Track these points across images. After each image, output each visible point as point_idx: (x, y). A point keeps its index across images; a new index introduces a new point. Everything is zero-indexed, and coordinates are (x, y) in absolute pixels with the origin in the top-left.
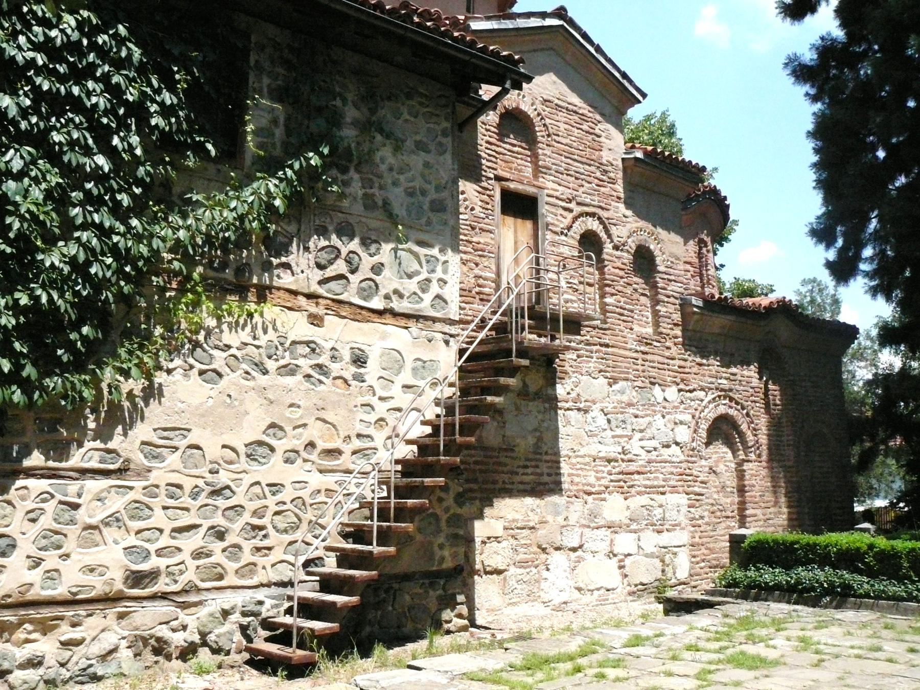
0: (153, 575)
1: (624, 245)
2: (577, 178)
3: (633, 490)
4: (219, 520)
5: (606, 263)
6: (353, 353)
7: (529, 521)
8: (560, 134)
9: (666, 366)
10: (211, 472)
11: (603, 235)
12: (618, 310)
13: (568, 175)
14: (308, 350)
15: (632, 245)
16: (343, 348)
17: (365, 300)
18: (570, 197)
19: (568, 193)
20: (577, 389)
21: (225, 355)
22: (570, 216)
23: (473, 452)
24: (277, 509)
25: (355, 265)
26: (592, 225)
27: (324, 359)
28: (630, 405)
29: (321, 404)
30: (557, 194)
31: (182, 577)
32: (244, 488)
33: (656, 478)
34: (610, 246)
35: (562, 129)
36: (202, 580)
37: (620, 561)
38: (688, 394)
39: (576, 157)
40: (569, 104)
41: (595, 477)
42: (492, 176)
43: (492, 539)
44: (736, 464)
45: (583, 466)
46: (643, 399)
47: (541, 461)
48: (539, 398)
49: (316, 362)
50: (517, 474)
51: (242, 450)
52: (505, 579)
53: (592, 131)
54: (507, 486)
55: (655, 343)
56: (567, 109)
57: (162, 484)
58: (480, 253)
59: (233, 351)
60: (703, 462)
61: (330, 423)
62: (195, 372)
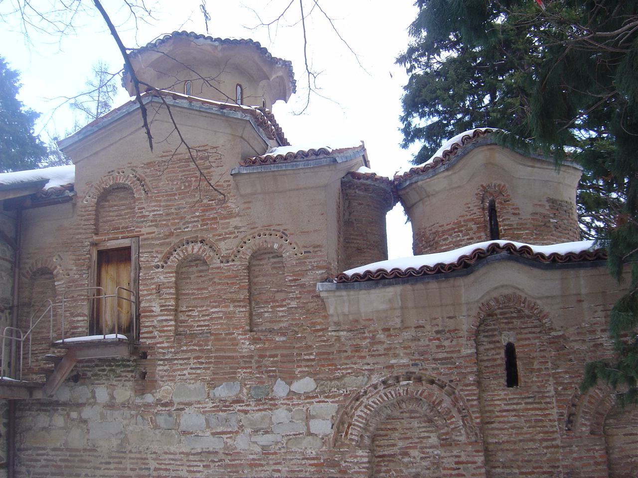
19: (166, 231)
22: (166, 249)
23: (59, 452)
26: (193, 249)
28: (239, 401)
33: (279, 471)
34: (219, 261)
41: (188, 471)
45: (172, 462)
48: (124, 407)
50: (100, 469)
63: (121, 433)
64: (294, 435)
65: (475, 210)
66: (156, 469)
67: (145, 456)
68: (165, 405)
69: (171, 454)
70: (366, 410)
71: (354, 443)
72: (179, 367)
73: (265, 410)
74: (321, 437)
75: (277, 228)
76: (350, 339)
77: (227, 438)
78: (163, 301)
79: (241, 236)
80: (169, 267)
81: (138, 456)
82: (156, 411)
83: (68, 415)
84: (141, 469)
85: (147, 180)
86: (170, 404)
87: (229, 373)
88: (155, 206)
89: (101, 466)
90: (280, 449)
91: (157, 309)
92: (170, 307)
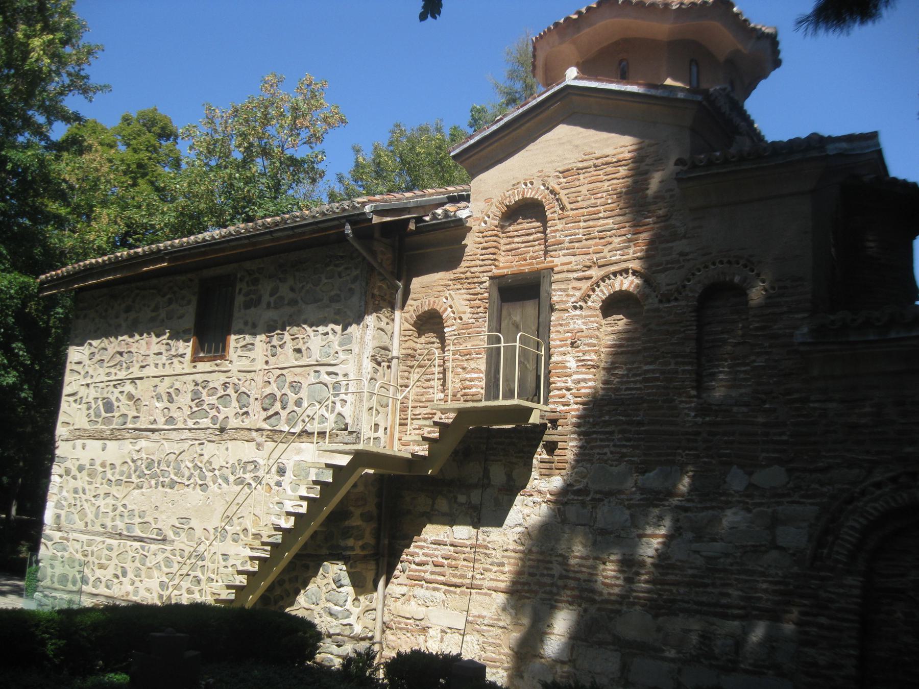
2: (600, 239)
8: (579, 199)
13: (587, 240)
18: (588, 264)
20: (585, 481)
21: (211, 474)
22: (589, 283)
26: (622, 284)
30: (569, 267)
34: (656, 300)
39: (601, 215)
40: (597, 159)
43: (453, 630)
50: (490, 570)
55: (735, 409)
56: (595, 166)
57: (178, 549)
63: (520, 525)
64: (753, 546)
67: (548, 558)
70: (861, 520)
71: (840, 566)
72: (598, 443)
73: (712, 508)
74: (791, 552)
78: (581, 354)
80: (590, 308)
83: (456, 498)
85: (563, 192)
88: (573, 228)
89: (491, 567)
90: (731, 565)
91: (572, 364)
92: (590, 363)
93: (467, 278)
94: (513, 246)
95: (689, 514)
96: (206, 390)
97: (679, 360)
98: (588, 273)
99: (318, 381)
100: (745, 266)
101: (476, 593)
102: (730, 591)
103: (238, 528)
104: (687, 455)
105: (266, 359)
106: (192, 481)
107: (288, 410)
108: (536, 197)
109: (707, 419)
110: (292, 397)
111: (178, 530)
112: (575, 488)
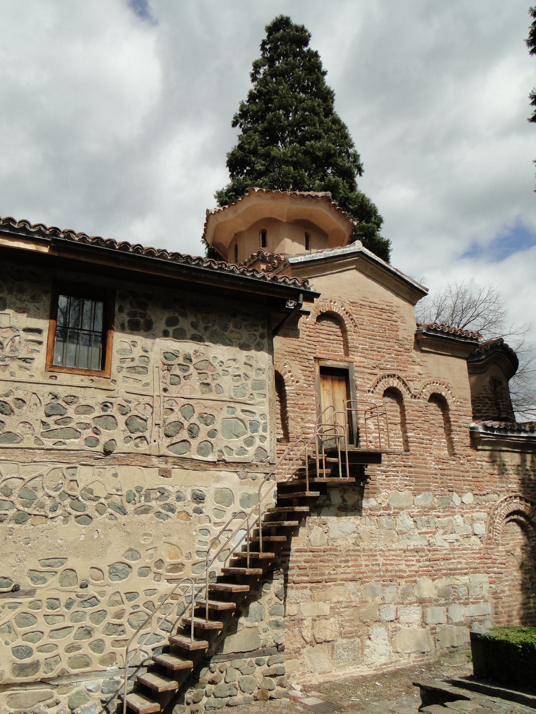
0: (35, 665)
1: (420, 395)
3: (439, 573)
4: (87, 622)
5: (406, 408)
6: (194, 494)
7: (351, 602)
8: (364, 323)
9: (462, 478)
10: (81, 587)
11: (402, 389)
12: (417, 441)
14: (158, 494)
15: (427, 393)
16: (186, 491)
17: (203, 455)
20: (387, 501)
21: (95, 504)
22: (374, 379)
24: (133, 611)
25: (194, 431)
26: (393, 383)
27: (172, 500)
28: (433, 508)
29: (167, 532)
30: (364, 364)
31: (57, 666)
32: (107, 597)
34: (409, 396)
35: (366, 320)
36: (73, 668)
37: (432, 629)
38: (483, 497)
39: (378, 338)
41: (406, 565)
42: (312, 358)
44: (532, 547)
45: (395, 558)
46: (443, 504)
47: (359, 556)
49: (165, 502)
50: (340, 567)
51: (106, 569)
52: (333, 648)
53: (389, 318)
54: (332, 577)
55: (451, 462)
58: (305, 411)
59: (103, 500)
60: (501, 548)
61: (175, 545)
62: (73, 517)
63: (354, 532)
65: (489, 392)
66: (384, 565)
67: (374, 553)
68: (385, 509)
69: (393, 550)
75: (444, 380)
76: (488, 469)
77: (429, 537)
79: (423, 380)
80: (377, 393)
81: (370, 553)
82: (379, 513)
84: (373, 565)
86: (388, 508)
87: (426, 485)
91: (372, 426)
93: (298, 353)
94: (320, 339)
95: (439, 519)
96: (74, 406)
97: (424, 432)
98: (375, 371)
99: (233, 416)
100: (446, 387)
101: (334, 585)
102: (461, 560)
103: (148, 561)
104: (435, 486)
105: (165, 386)
106: (59, 512)
107: (199, 439)
108: (339, 313)
109: (440, 466)
110: (204, 430)
111: (42, 575)
112: (383, 506)
